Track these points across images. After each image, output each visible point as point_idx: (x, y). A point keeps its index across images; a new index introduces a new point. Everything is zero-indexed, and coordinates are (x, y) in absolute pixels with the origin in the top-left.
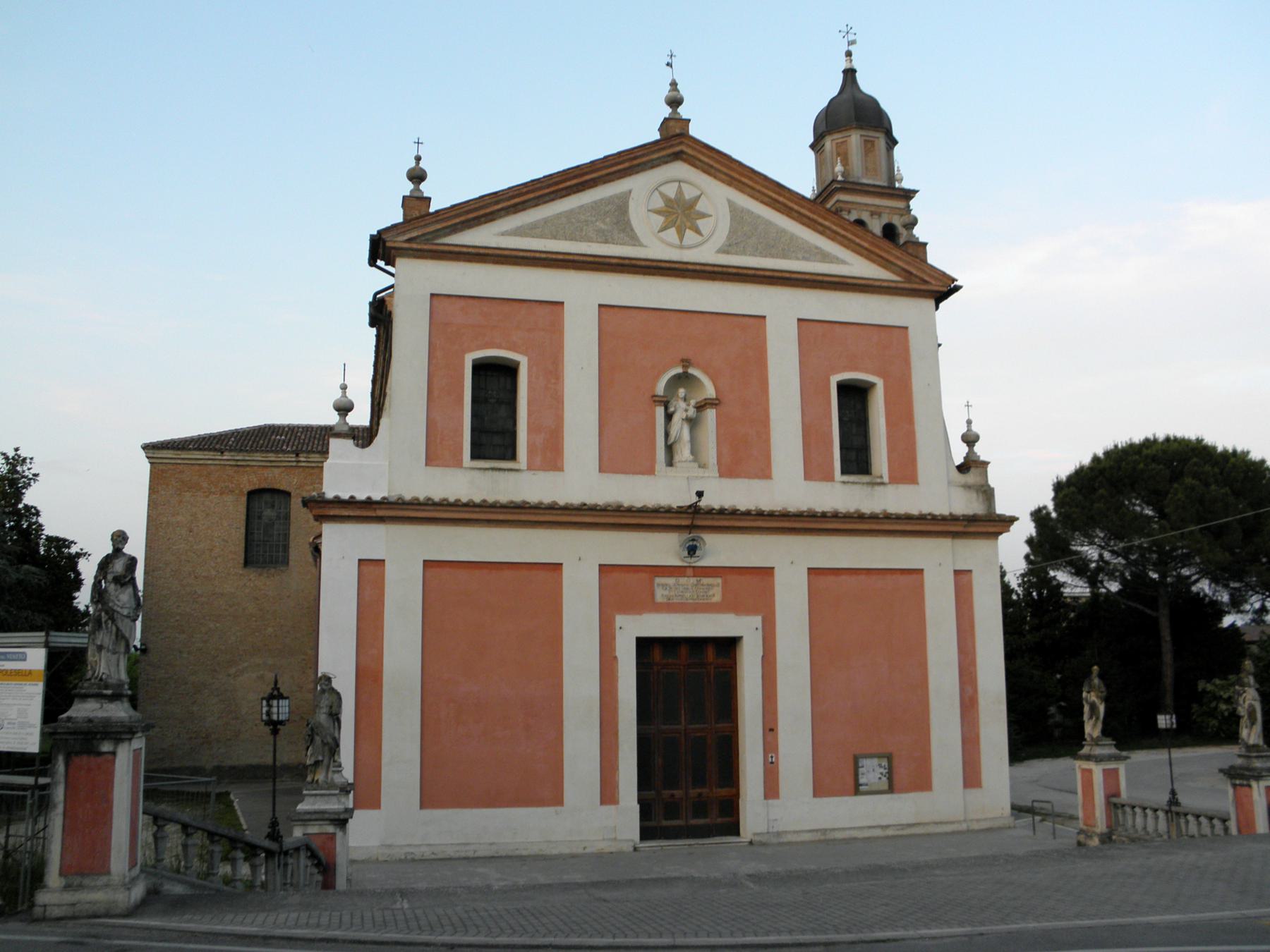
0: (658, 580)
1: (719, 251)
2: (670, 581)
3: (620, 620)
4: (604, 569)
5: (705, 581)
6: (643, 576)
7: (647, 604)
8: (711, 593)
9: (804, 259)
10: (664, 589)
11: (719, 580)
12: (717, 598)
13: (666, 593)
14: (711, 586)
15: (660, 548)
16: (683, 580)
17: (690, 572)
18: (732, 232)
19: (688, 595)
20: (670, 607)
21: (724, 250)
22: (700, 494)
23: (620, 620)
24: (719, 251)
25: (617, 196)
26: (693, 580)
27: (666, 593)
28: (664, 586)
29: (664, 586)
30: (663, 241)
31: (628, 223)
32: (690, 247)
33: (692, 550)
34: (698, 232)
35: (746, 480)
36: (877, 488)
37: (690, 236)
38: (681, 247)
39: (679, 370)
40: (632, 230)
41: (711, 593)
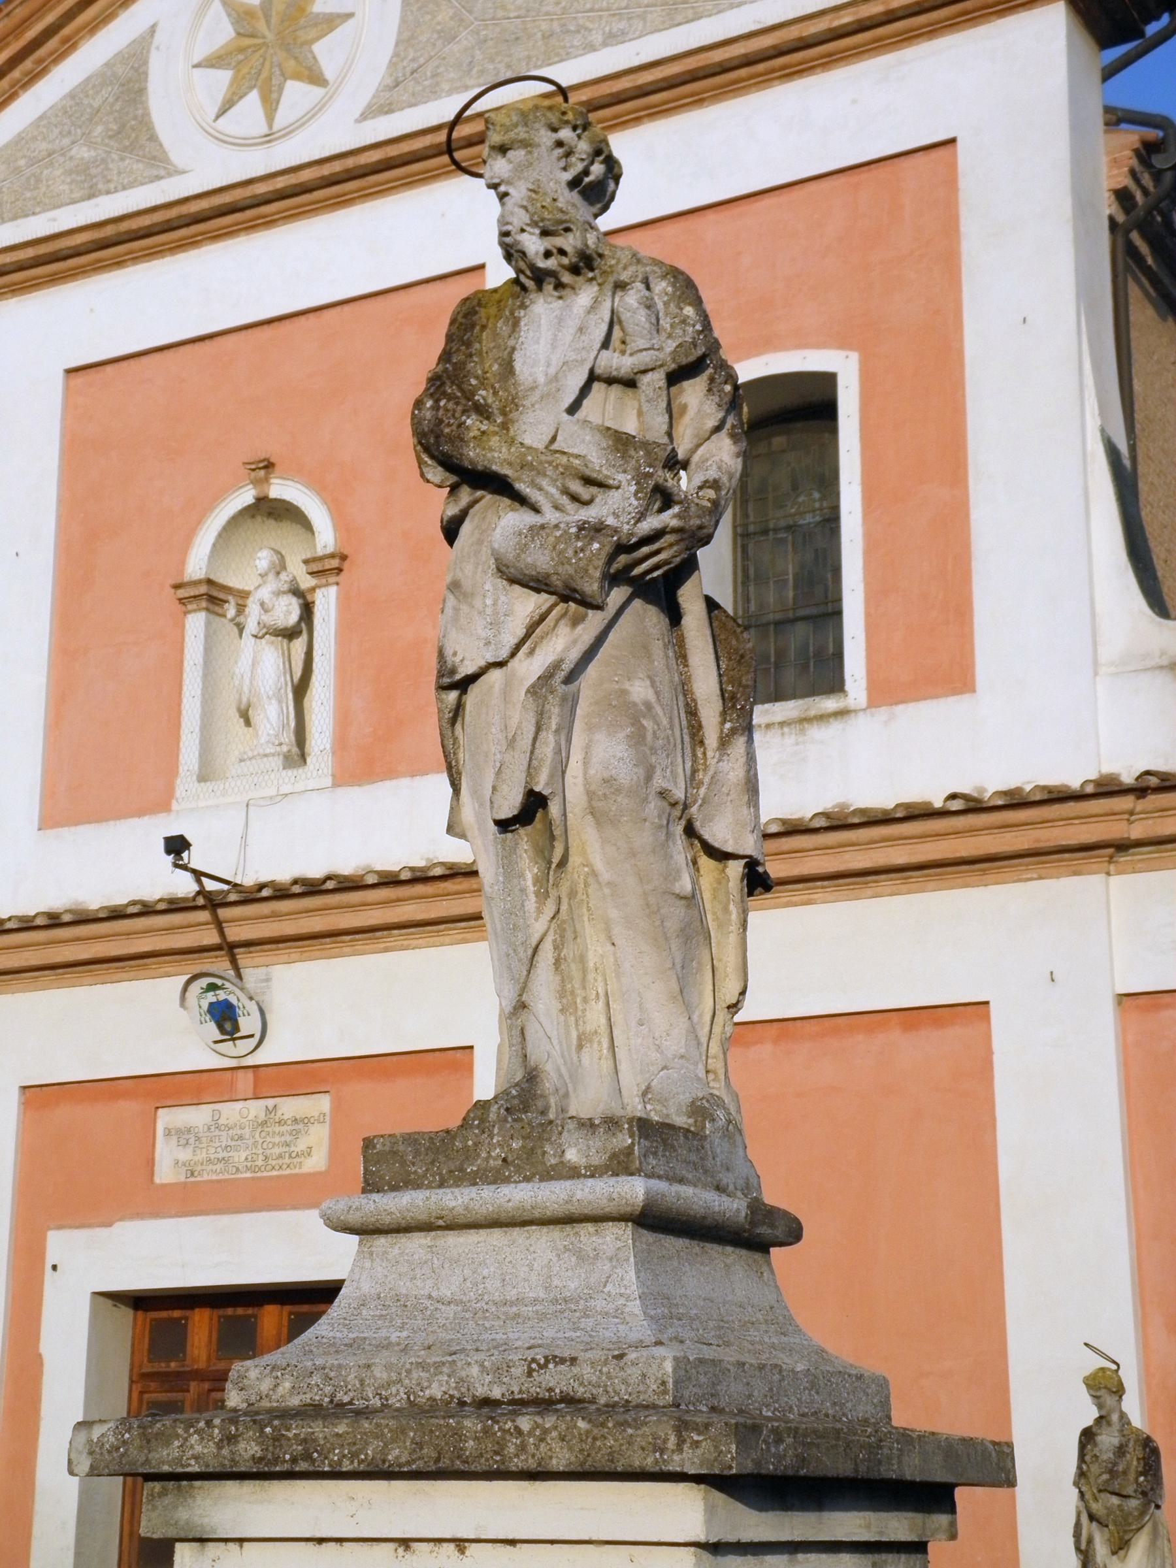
0: (166, 1118)
1: (364, 117)
2: (196, 1117)
3: (59, 1244)
4: (39, 1097)
5: (290, 1107)
6: (128, 1108)
7: (132, 1192)
8: (301, 1145)
9: (612, 39)
10: (178, 1143)
11: (324, 1103)
12: (317, 1162)
13: (184, 1155)
14: (306, 1121)
15: (145, 1024)
16: (231, 1112)
17: (245, 1082)
18: (406, 40)
19: (240, 1157)
20: (194, 1199)
21: (380, 108)
22: (177, 846)
23: (59, 1244)
24: (364, 117)
25: (121, 57)
26: (256, 1108)
27: (184, 1155)
28: (182, 1135)
29: (182, 1135)
30: (223, 140)
31: (145, 123)
32: (289, 131)
33: (224, 1017)
34: (316, 78)
35: (405, 782)
36: (816, 732)
37: (296, 95)
38: (269, 138)
39: (246, 497)
40: (153, 138)
41: (301, 1145)
